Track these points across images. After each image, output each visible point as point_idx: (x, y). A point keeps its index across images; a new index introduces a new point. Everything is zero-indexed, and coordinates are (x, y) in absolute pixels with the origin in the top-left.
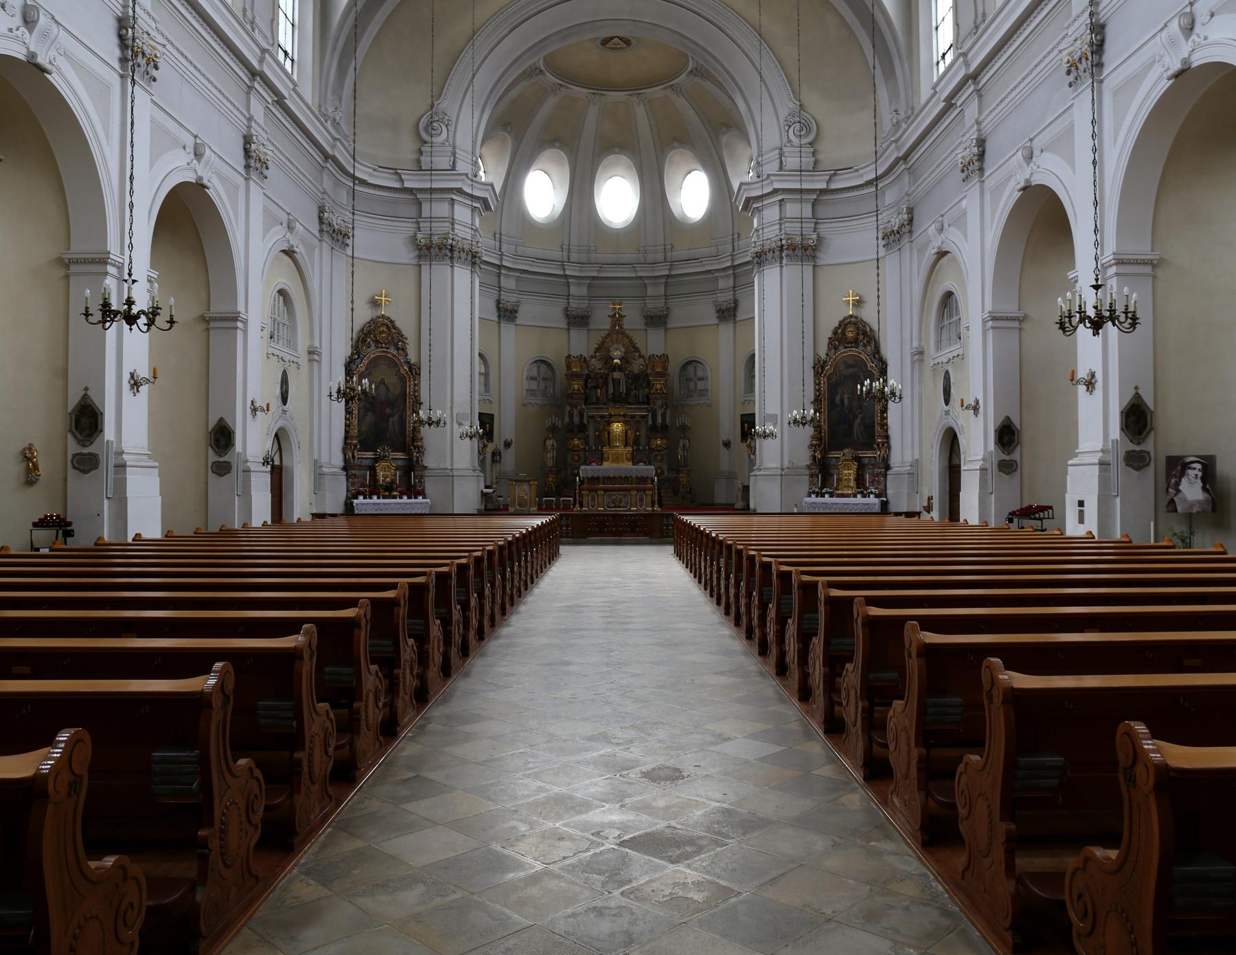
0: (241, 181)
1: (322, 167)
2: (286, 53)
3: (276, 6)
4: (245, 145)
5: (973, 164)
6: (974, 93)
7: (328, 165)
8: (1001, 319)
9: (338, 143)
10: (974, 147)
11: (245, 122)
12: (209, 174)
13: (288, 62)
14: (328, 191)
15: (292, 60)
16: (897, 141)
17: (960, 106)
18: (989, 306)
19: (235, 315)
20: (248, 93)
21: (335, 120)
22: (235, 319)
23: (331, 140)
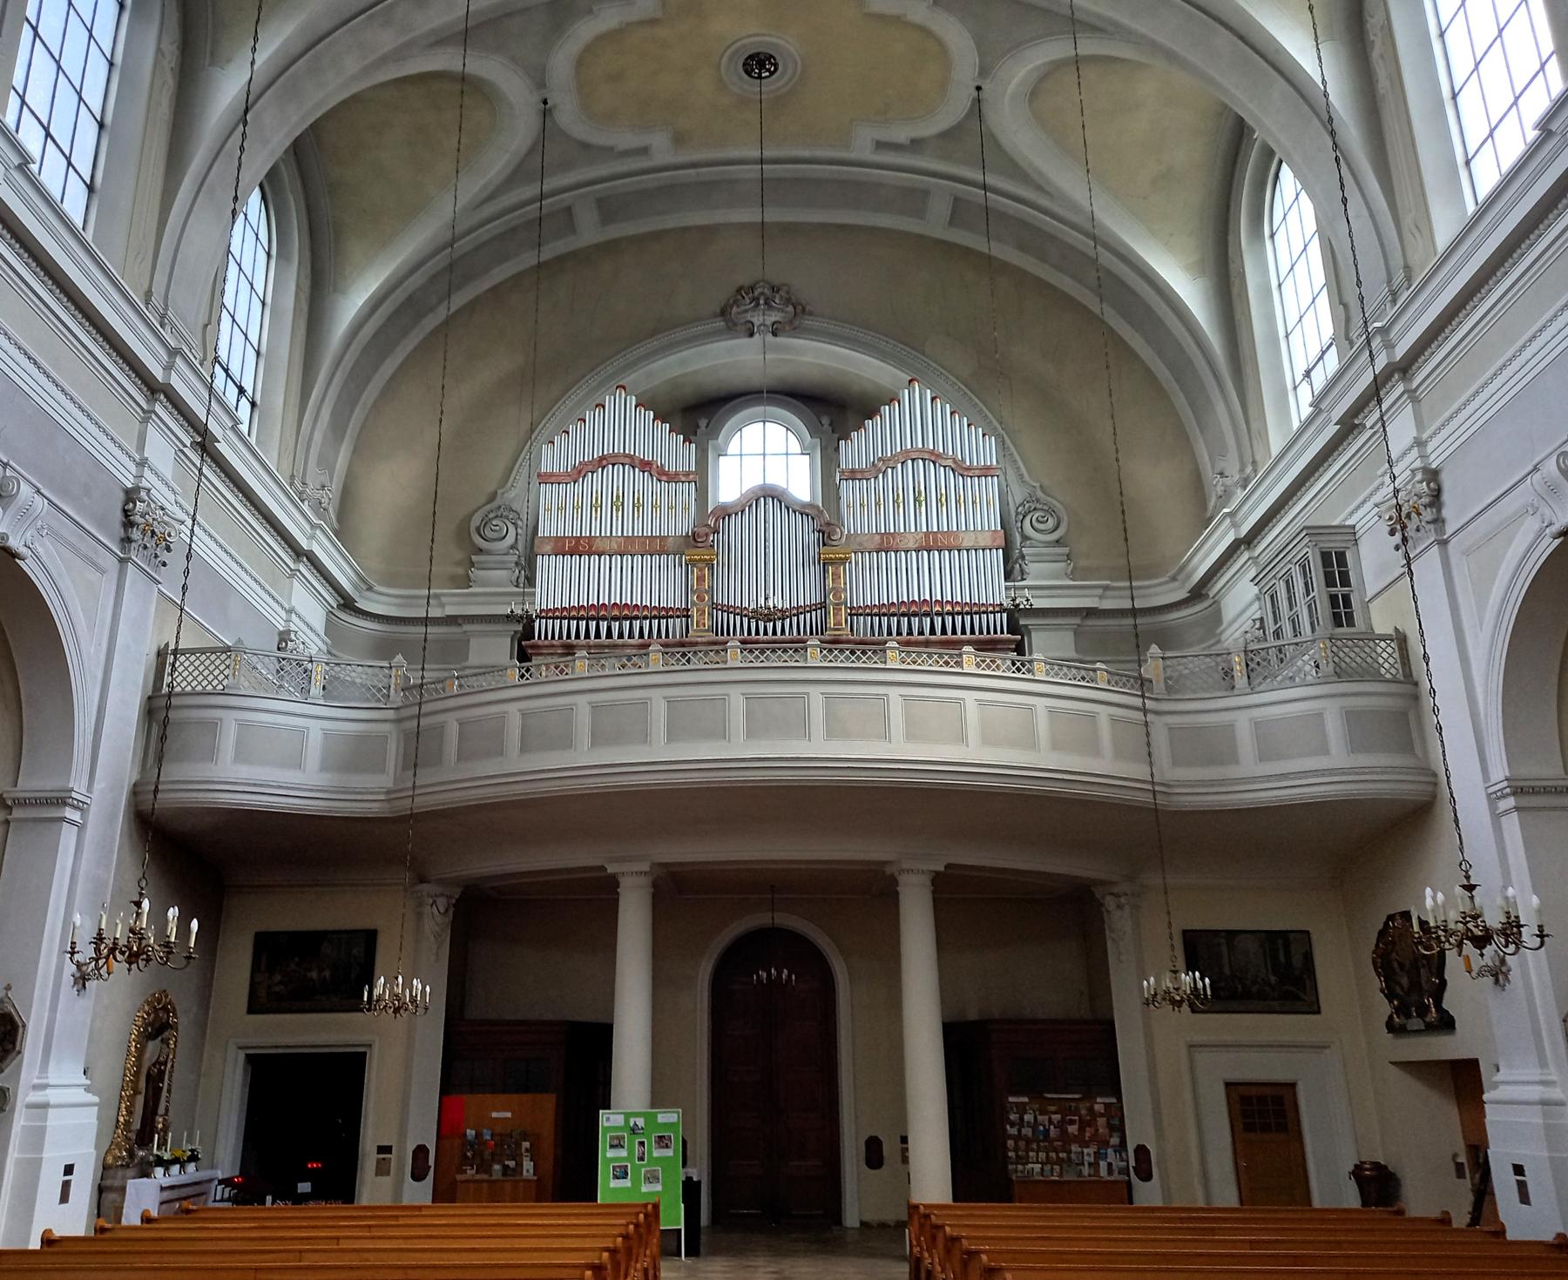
0: (111, 563)
1: (291, 570)
2: (241, 391)
3: (217, 304)
4: (126, 503)
5: (1419, 514)
6: (1406, 396)
7: (302, 568)
8: (1534, 791)
9: (318, 532)
10: (1421, 482)
11: (133, 468)
12: (28, 534)
13: (245, 405)
14: (299, 609)
15: (253, 404)
16: (1232, 515)
17: (1371, 428)
18: (1499, 771)
19: (63, 795)
20: (145, 421)
21: (320, 503)
22: (62, 801)
23: (308, 527)
